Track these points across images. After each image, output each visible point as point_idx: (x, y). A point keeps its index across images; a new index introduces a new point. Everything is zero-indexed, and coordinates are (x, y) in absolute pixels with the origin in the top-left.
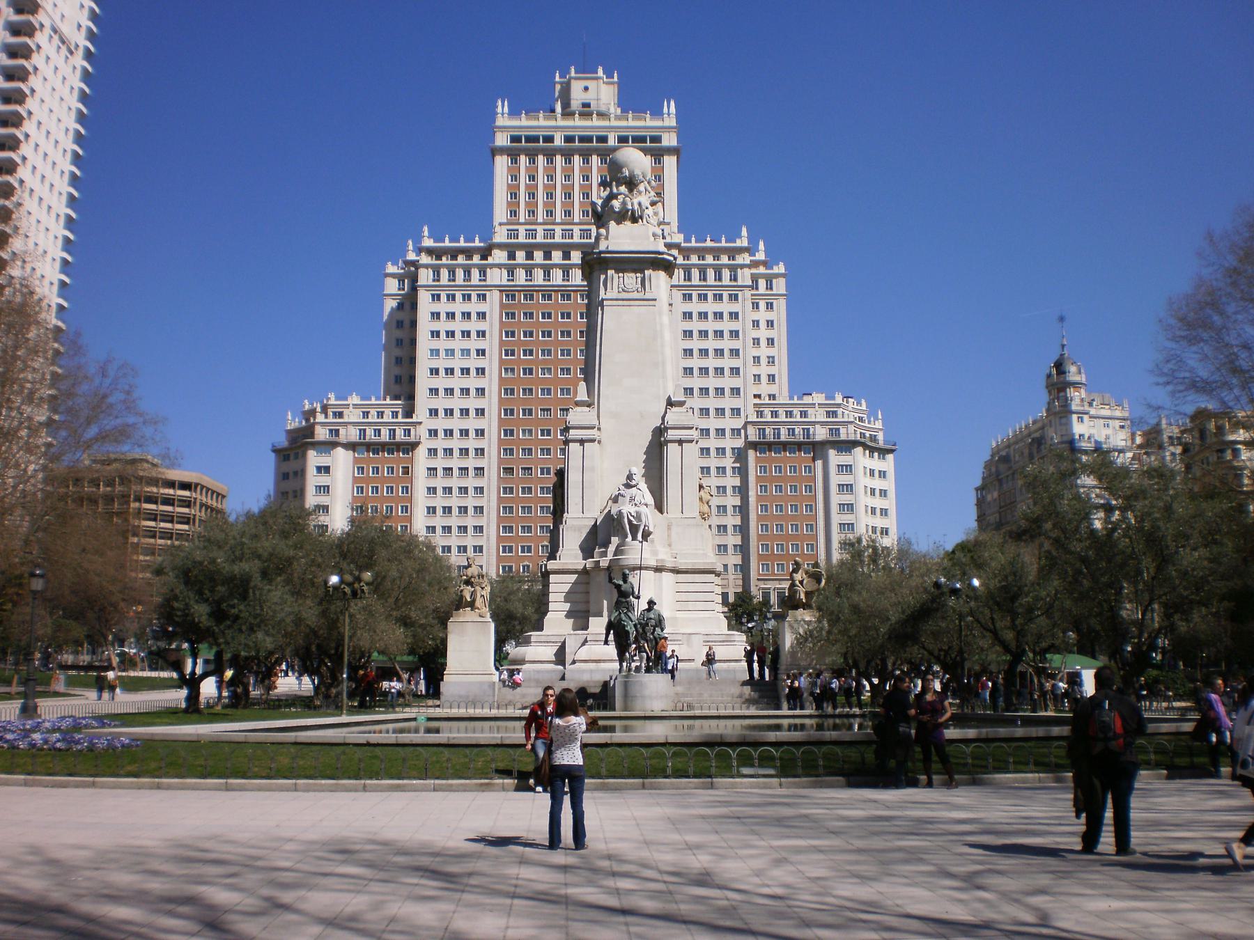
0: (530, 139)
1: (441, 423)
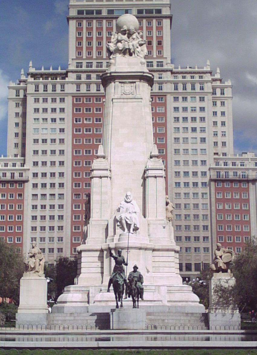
0: (88, 12)
1: (40, 170)
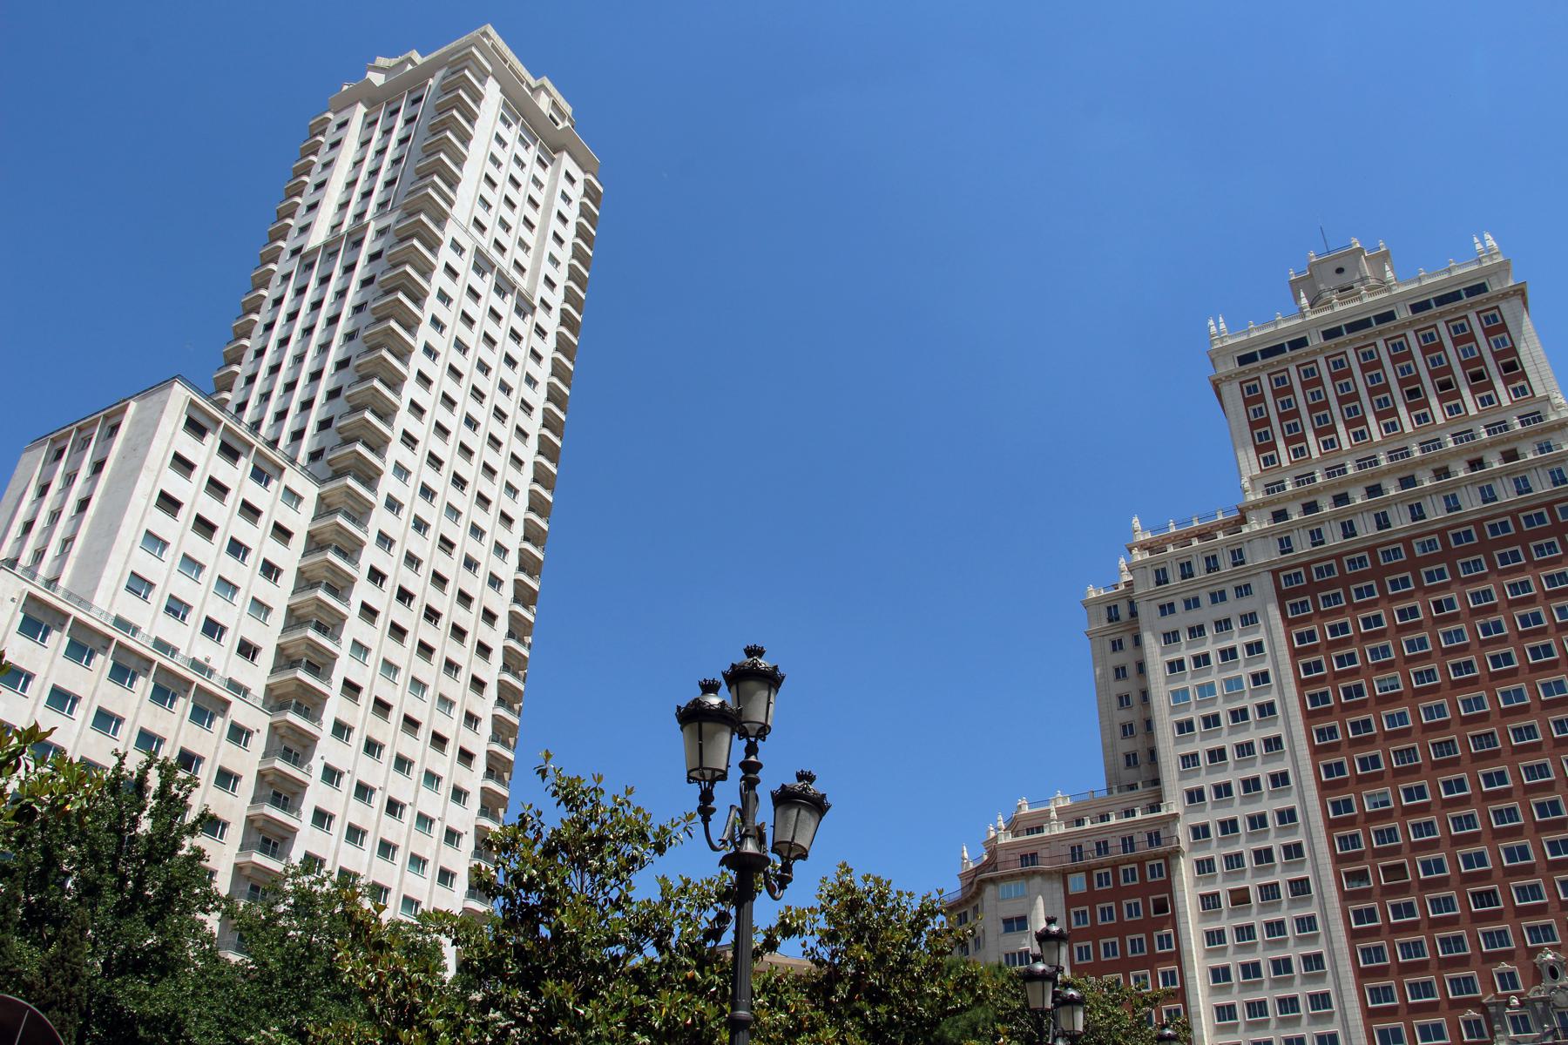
1: (1211, 815)
